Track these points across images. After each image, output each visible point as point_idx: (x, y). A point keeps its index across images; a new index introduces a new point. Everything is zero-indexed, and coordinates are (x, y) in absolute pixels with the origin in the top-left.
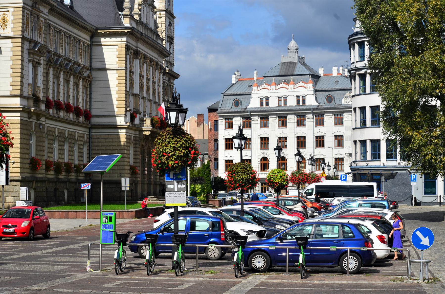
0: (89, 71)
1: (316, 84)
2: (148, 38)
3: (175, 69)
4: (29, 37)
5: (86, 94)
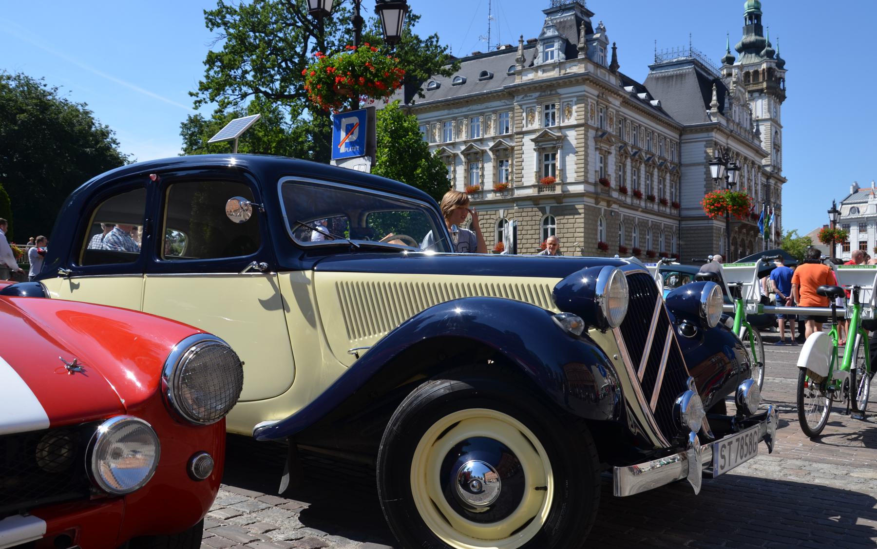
5: (676, 189)
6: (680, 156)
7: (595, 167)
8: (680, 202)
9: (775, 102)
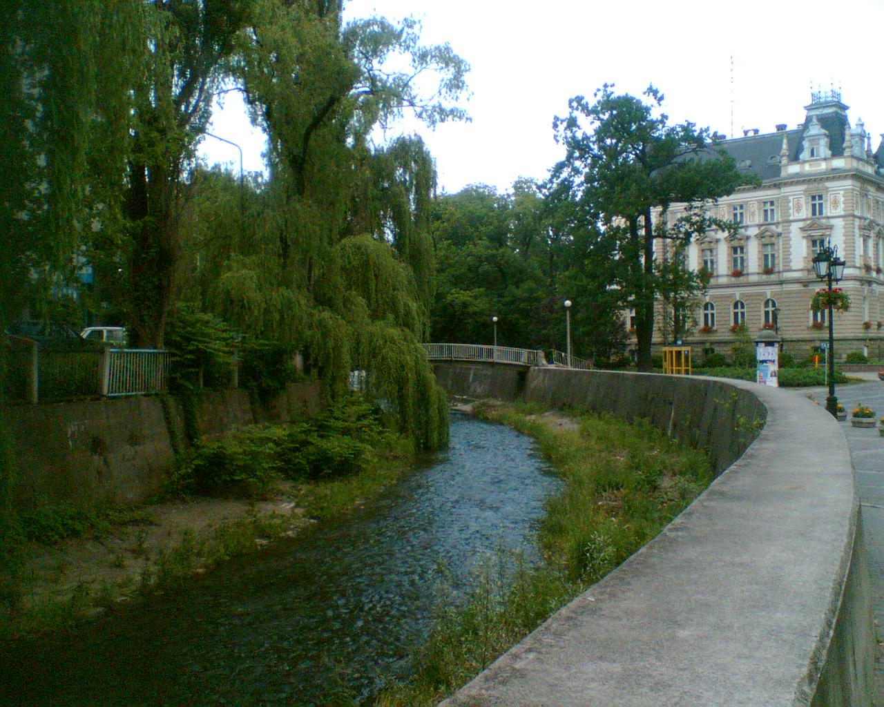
4: (859, 215)
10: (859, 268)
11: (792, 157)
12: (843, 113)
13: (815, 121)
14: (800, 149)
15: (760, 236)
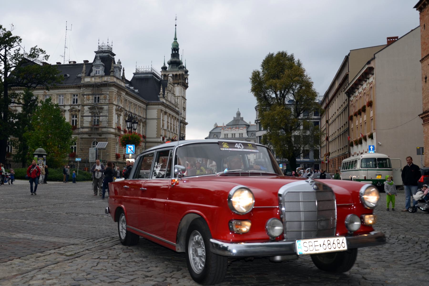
0: (145, 120)
1: (247, 128)
2: (171, 106)
3: (186, 121)
4: (116, 104)
5: (144, 129)
6: (146, 115)
7: (115, 121)
8: (146, 135)
9: (184, 88)
10: (115, 129)
11: (87, 74)
12: (112, 57)
13: (99, 58)
14: (91, 71)
15: (70, 111)
